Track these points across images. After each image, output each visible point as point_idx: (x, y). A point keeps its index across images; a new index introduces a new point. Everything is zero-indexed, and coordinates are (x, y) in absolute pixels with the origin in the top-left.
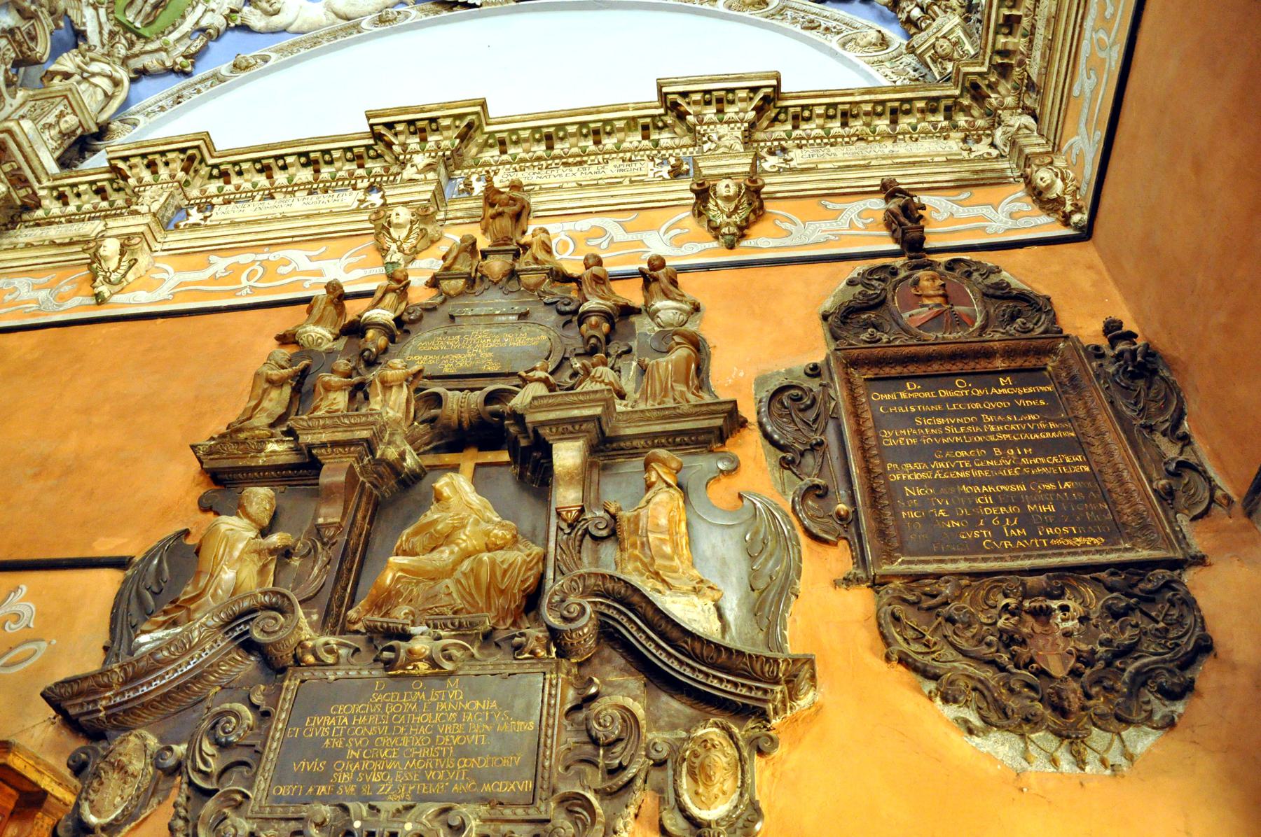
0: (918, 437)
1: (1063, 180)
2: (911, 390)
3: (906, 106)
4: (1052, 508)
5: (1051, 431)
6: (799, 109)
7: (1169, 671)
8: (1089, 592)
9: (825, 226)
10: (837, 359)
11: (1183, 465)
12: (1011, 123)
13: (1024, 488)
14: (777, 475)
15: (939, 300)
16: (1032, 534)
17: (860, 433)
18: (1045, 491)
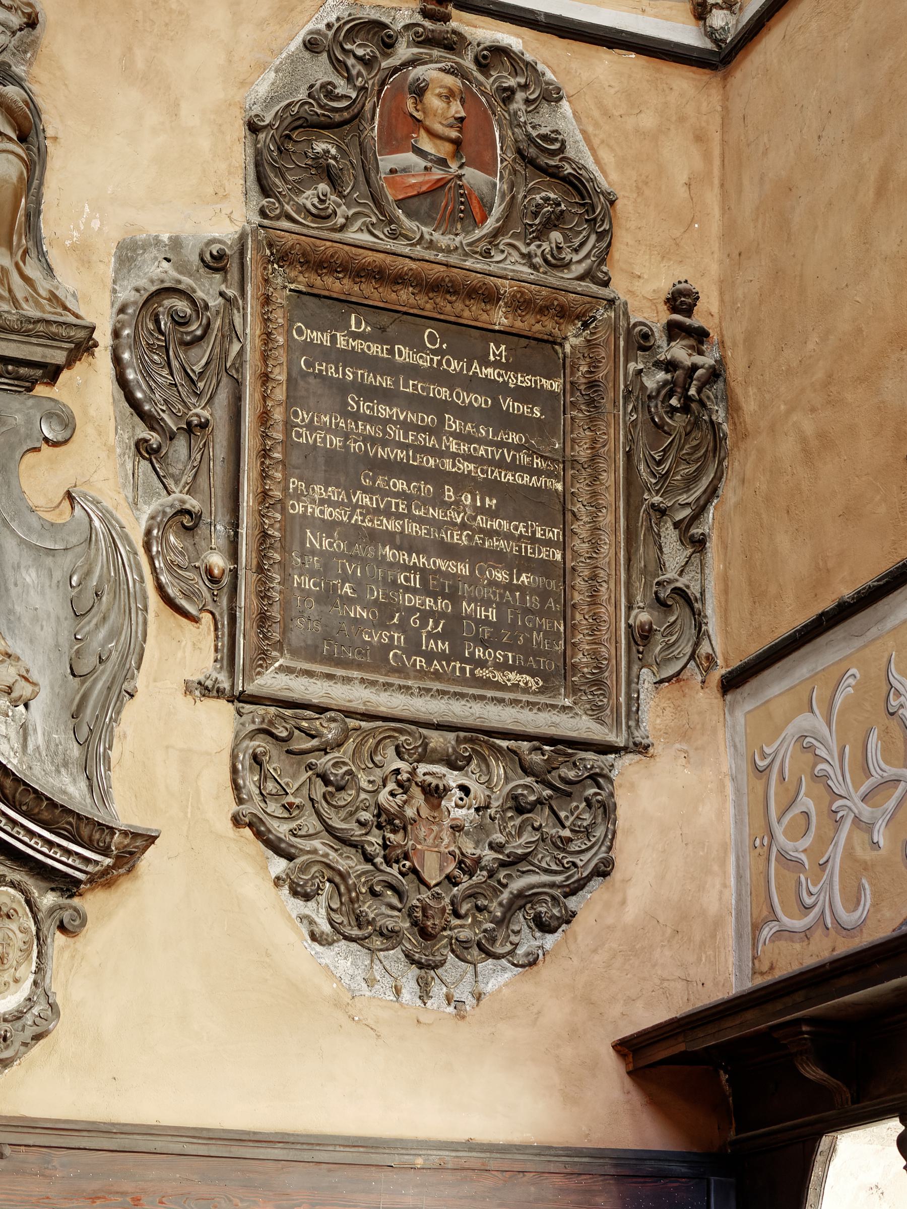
0: (346, 436)
2: (353, 335)
4: (492, 615)
5: (533, 472)
7: (554, 898)
8: (499, 770)
10: (258, 247)
14: (129, 466)
15: (444, 150)
16: (456, 655)
17: (264, 418)
18: (493, 583)
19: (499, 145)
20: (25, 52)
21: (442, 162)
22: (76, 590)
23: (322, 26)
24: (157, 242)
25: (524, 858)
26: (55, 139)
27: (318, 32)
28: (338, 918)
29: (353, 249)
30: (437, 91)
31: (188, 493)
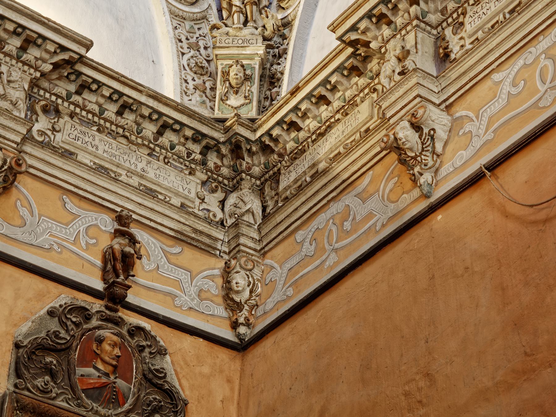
1: (251, 292)
3: (177, 127)
6: (90, 80)
9: (56, 229)
10: (11, 402)
12: (246, 199)
15: (109, 369)
19: (134, 371)
21: (107, 375)
23: (57, 305)
27: (55, 308)
29: (59, 410)
30: (109, 342)
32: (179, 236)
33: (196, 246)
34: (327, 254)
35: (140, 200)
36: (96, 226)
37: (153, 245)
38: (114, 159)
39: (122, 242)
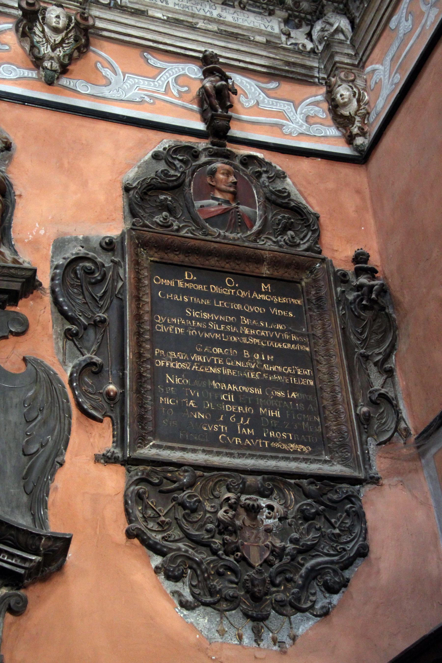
0: (186, 327)
1: (359, 101)
2: (187, 281)
5: (292, 342)
7: (335, 571)
8: (291, 496)
9: (144, 83)
10: (131, 238)
11: (383, 396)
12: (332, 20)
13: (260, 392)
14: (61, 344)
15: (228, 197)
16: (258, 435)
17: (138, 317)
18: (276, 397)
19: (256, 196)
20: (5, 161)
21: (227, 202)
22: (27, 408)
23: (161, 149)
24: (76, 239)
25: (312, 547)
26: (20, 196)
27: (159, 151)
28: (197, 591)
29: (183, 239)
30: (222, 172)
31: (95, 355)
32: (272, 71)
33: (292, 78)
34: (426, 15)
35: (223, 44)
36: (184, 75)
37: (247, 84)
38: (187, 10)
39: (212, 79)
